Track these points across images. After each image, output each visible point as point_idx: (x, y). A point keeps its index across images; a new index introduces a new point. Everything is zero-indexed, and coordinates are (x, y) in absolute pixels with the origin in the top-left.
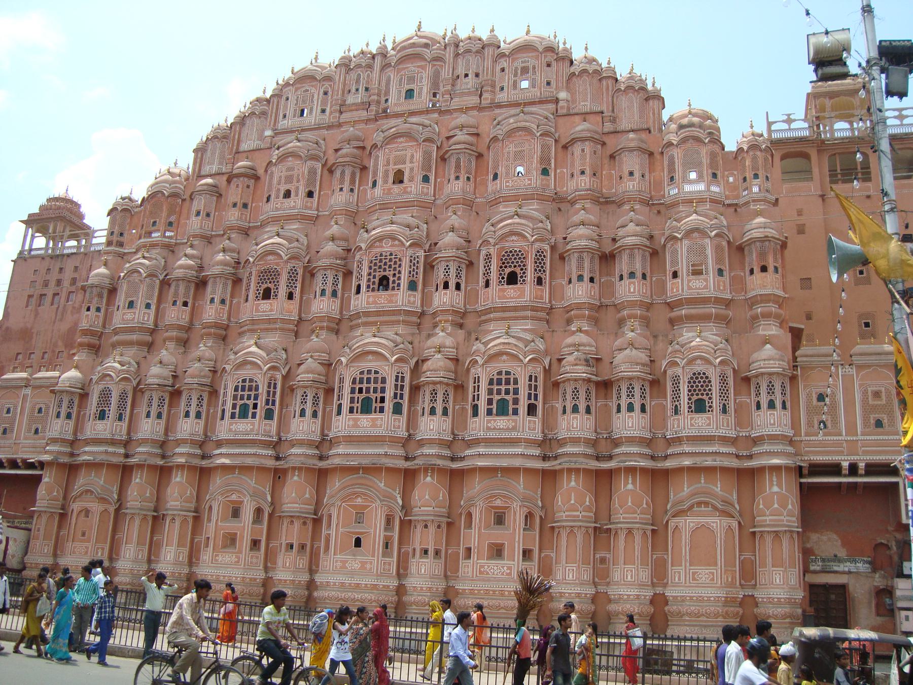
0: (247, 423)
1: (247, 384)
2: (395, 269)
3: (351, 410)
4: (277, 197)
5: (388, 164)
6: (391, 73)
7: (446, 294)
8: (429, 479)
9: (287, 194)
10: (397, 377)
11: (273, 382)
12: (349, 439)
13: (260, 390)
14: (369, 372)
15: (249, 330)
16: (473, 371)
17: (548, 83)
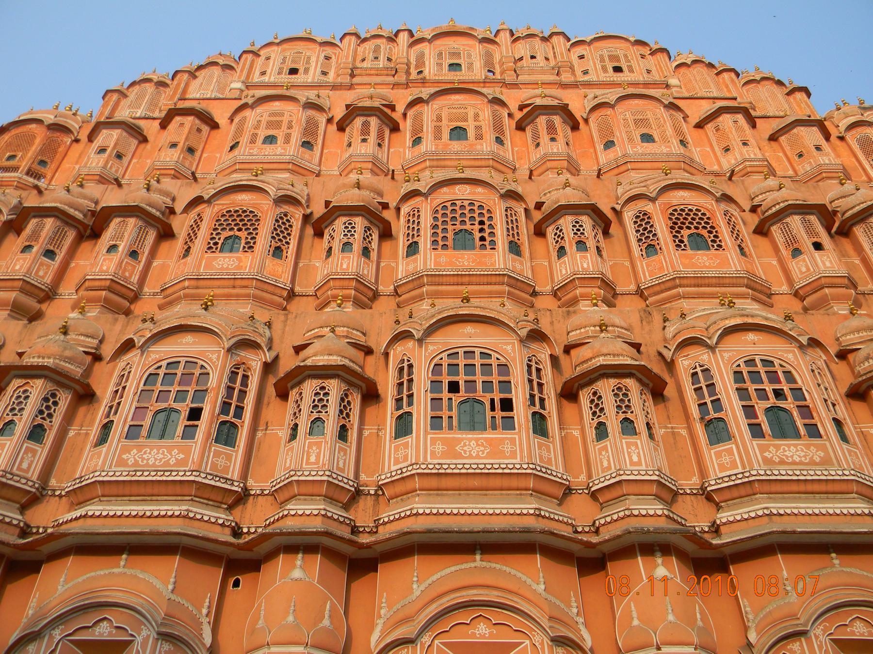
0: (170, 449)
1: (179, 372)
2: (482, 223)
3: (436, 422)
4: (253, 142)
5: (439, 119)
6: (424, 47)
7: (586, 257)
8: (661, 571)
9: (270, 140)
10: (529, 366)
11: (241, 372)
12: (434, 482)
13: (213, 381)
14: (469, 354)
15: (186, 296)
16: (684, 364)
17: (649, 72)
